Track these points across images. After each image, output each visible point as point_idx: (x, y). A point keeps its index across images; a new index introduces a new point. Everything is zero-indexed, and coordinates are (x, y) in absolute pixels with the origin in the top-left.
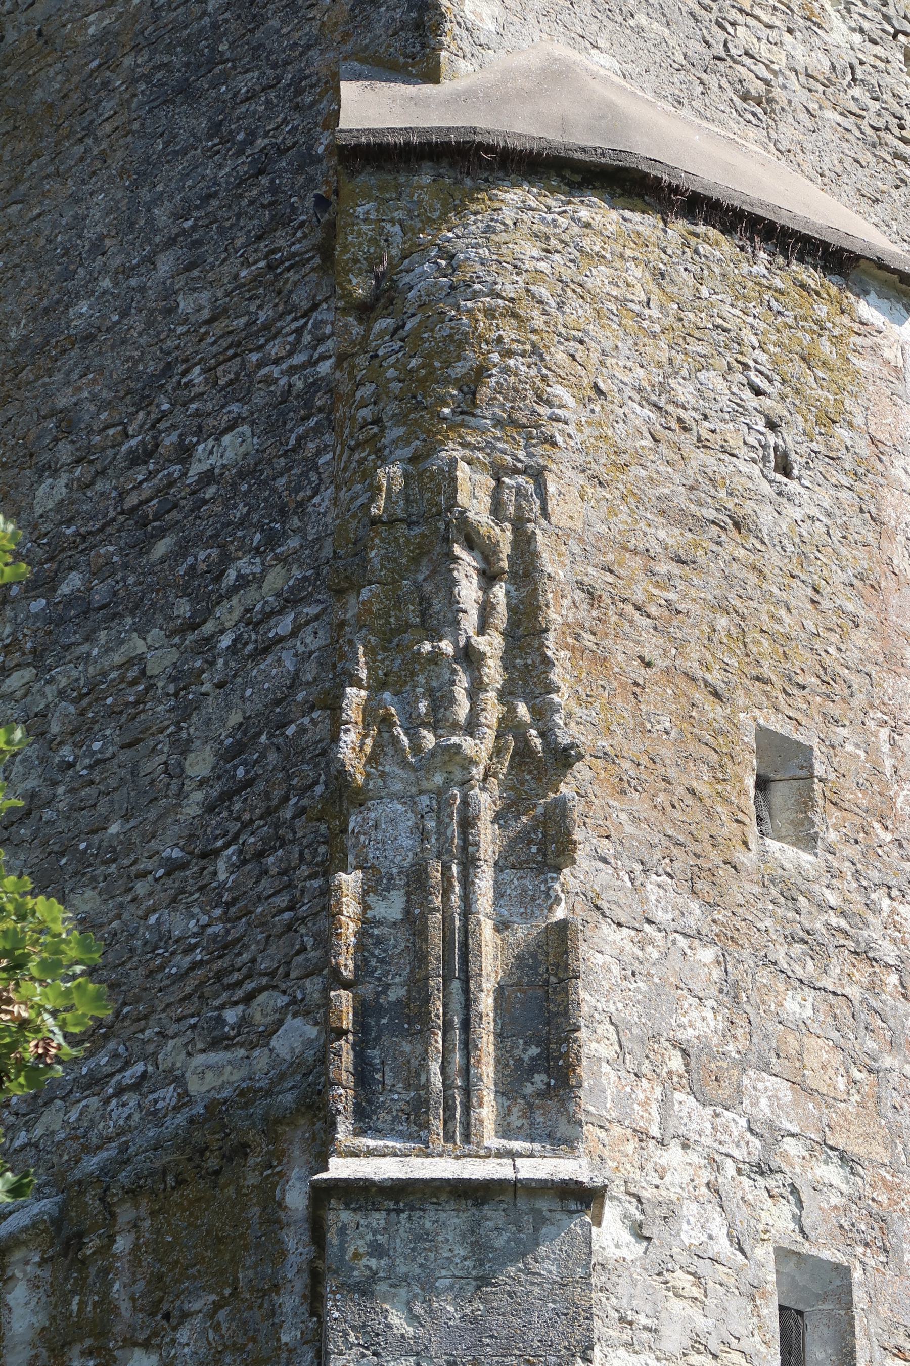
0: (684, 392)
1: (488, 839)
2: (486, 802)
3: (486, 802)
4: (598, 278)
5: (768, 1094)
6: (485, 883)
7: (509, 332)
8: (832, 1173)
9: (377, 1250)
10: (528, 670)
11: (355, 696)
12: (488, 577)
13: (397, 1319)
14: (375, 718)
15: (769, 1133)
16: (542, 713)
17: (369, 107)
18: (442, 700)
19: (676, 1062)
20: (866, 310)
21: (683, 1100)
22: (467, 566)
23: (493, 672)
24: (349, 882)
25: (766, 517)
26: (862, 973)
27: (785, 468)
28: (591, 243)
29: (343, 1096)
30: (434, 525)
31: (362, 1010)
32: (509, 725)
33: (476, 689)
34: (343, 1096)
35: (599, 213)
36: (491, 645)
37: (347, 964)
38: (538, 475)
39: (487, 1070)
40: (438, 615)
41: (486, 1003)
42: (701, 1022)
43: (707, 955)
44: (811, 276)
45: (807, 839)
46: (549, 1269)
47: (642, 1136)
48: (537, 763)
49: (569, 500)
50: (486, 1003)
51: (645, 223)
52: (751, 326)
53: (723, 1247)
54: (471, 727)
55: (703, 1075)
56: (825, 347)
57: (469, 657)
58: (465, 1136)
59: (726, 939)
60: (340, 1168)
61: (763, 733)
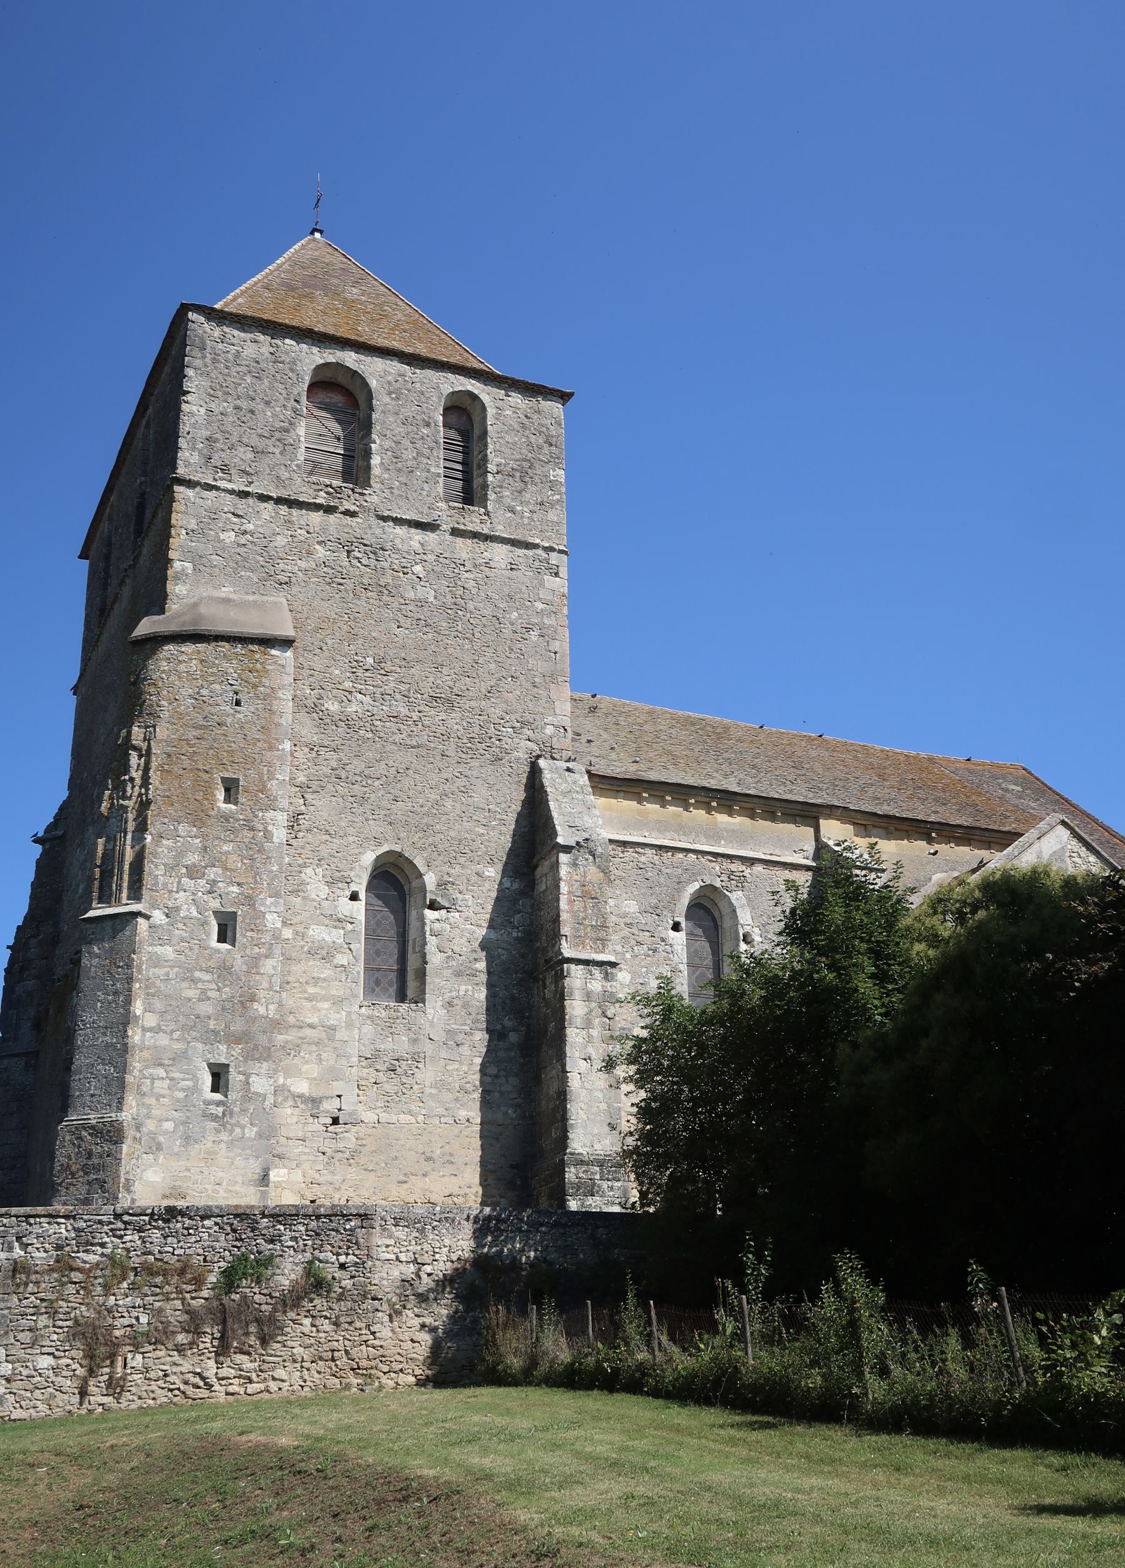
0: (204, 692)
1: (131, 826)
2: (131, 816)
3: (131, 816)
4: (182, 667)
5: (212, 873)
6: (129, 837)
7: (152, 690)
8: (235, 889)
9: (93, 933)
10: (146, 781)
11: (107, 793)
12: (140, 756)
13: (96, 949)
14: (111, 798)
15: (214, 882)
16: (147, 790)
17: (146, 627)
18: (125, 791)
19: (184, 871)
20: (274, 652)
21: (185, 880)
22: (134, 755)
23: (138, 781)
24: (101, 841)
25: (229, 720)
26: (250, 834)
27: (238, 703)
28: (184, 657)
29: (95, 895)
30: (128, 745)
31: (102, 873)
32: (140, 795)
33: (133, 787)
34: (95, 895)
35: (189, 648)
36: (137, 775)
37: (99, 862)
38: (154, 726)
39: (125, 885)
40: (126, 769)
41: (126, 867)
42: (193, 858)
43: (198, 841)
44: (255, 648)
45: (236, 804)
46: (127, 933)
47: (171, 892)
48: (144, 805)
49: (162, 732)
50: (126, 867)
51: (201, 647)
52: (231, 668)
53: (195, 914)
54: (130, 798)
55: (193, 872)
56: (258, 666)
57: (132, 779)
58: (118, 902)
59: (204, 837)
60: (91, 914)
61: (222, 778)
